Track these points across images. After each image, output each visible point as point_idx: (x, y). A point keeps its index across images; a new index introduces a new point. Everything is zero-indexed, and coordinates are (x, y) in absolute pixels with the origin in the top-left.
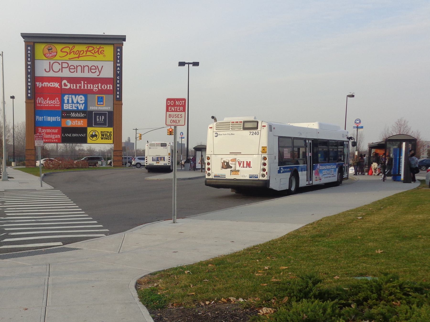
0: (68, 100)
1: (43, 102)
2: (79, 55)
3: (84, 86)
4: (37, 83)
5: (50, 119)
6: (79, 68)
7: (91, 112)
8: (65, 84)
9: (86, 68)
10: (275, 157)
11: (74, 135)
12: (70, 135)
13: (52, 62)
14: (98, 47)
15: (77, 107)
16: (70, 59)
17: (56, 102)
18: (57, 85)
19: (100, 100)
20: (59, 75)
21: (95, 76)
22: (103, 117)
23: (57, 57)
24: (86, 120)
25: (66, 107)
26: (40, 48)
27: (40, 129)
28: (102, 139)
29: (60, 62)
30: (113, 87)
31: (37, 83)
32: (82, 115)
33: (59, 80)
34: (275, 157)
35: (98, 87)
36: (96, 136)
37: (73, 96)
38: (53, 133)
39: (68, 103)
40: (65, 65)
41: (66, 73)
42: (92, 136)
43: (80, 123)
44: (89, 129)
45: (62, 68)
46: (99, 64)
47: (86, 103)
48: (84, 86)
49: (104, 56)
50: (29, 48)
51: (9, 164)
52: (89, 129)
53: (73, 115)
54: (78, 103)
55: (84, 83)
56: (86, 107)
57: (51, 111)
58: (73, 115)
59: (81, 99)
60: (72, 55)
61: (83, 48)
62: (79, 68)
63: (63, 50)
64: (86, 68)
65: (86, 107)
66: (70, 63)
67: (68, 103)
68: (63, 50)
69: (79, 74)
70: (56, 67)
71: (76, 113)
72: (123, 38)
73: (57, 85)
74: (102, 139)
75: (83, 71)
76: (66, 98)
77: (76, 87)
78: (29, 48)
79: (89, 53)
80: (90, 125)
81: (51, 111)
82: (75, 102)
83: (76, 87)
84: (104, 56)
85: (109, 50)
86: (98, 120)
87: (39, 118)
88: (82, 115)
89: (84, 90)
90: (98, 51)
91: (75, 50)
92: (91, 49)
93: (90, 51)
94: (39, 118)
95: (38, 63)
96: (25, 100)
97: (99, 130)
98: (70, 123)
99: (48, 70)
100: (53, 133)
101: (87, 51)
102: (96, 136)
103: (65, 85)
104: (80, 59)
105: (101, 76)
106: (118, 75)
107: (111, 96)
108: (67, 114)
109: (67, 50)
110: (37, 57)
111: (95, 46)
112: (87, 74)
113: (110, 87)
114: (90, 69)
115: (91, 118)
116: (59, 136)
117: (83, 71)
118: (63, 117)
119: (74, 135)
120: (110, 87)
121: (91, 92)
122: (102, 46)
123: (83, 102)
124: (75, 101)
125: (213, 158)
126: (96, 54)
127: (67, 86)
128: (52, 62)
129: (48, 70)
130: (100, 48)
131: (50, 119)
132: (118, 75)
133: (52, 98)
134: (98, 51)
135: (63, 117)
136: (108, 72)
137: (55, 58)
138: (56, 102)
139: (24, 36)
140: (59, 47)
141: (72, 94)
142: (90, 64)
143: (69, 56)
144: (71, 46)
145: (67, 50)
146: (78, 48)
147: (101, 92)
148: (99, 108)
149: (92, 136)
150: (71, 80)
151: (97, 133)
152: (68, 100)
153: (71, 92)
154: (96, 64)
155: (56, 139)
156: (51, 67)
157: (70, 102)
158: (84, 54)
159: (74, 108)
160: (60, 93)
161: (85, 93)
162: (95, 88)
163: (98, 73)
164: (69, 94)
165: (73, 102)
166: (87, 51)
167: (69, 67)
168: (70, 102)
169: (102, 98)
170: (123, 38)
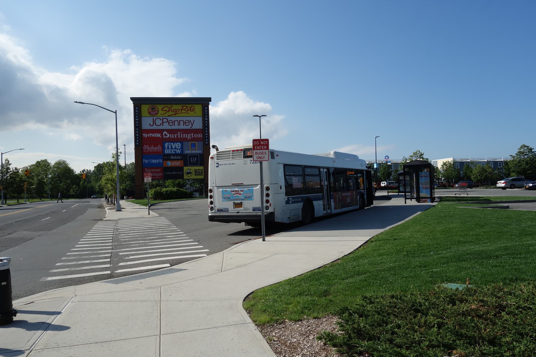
0: (168, 146)
1: (148, 149)
2: (176, 113)
3: (180, 136)
4: (144, 134)
5: (153, 161)
6: (176, 122)
7: (186, 155)
8: (165, 134)
9: (182, 122)
10: (281, 186)
11: (173, 173)
12: (170, 173)
13: (155, 118)
14: (190, 106)
15: (176, 152)
16: (169, 116)
17: (158, 148)
18: (159, 135)
19: (193, 146)
20: (161, 127)
21: (188, 127)
22: (196, 159)
23: (159, 115)
24: (182, 161)
25: (167, 152)
26: (145, 109)
27: (146, 170)
28: (195, 175)
29: (161, 118)
30: (203, 136)
31: (144, 134)
32: (180, 158)
33: (161, 131)
34: (281, 186)
35: (191, 136)
36: (190, 173)
37: (172, 144)
38: (157, 172)
39: (168, 148)
40: (165, 120)
41: (166, 126)
42: (188, 173)
43: (178, 164)
44: (185, 168)
45: (163, 122)
46: (192, 119)
47: (182, 148)
48: (180, 136)
49: (195, 113)
50: (137, 108)
51: (122, 198)
52: (185, 168)
53: (172, 157)
54: (175, 148)
55: (180, 134)
56: (182, 151)
57: (155, 155)
58: (172, 157)
59: (178, 145)
60: (170, 113)
61: (179, 107)
62: (176, 122)
63: (164, 109)
64: (182, 122)
65: (182, 151)
66: (169, 119)
67: (168, 148)
68: (164, 109)
69: (176, 127)
70: (158, 122)
71: (174, 156)
72: (209, 100)
73: (159, 135)
74: (195, 175)
75: (179, 124)
76: (166, 145)
77: (174, 136)
78: (137, 108)
79: (183, 111)
80: (186, 165)
81: (155, 155)
82: (174, 148)
83: (174, 136)
84: (195, 113)
85: (198, 108)
86: (192, 161)
87: (146, 161)
88: (180, 158)
89: (180, 138)
90: (190, 109)
91: (173, 109)
92: (184, 108)
93: (184, 109)
94: (146, 161)
95: (143, 119)
96: (134, 147)
97: (193, 168)
98: (169, 164)
99: (152, 124)
100: (157, 172)
101: (182, 110)
102: (190, 173)
103: (166, 135)
104: (177, 115)
105: (193, 128)
106: (206, 127)
107: (201, 143)
108: (167, 157)
109: (167, 109)
110: (143, 115)
111: (188, 106)
112: (182, 127)
113: (200, 136)
114: (184, 123)
115: (186, 159)
116: (161, 174)
117: (179, 124)
118: (164, 160)
119: (173, 173)
120: (200, 136)
121: (186, 140)
122: (193, 105)
123: (180, 147)
124: (174, 148)
125: (215, 190)
126: (189, 112)
127: (167, 136)
128: (155, 118)
129: (152, 124)
130: (192, 107)
131: (153, 161)
132: (206, 127)
133: (156, 146)
134: (190, 109)
135: (164, 160)
136: (198, 124)
137: (158, 115)
138: (158, 148)
139: (132, 99)
140: (160, 107)
141: (171, 142)
142: (184, 119)
143: (168, 114)
144: (169, 106)
145: (167, 109)
146: (175, 107)
147: (193, 139)
148: (193, 152)
149: (188, 173)
150: (170, 131)
151: (191, 171)
152: (168, 146)
153: (170, 140)
154: (189, 119)
155: (159, 176)
156: (154, 122)
157: (170, 147)
158: (180, 112)
159: (173, 152)
160: (162, 141)
161: (181, 141)
162: (189, 137)
163: (190, 125)
164: (169, 142)
165: (172, 148)
166: (182, 110)
167: (168, 122)
168: (170, 147)
169: (195, 144)
170: (209, 100)
